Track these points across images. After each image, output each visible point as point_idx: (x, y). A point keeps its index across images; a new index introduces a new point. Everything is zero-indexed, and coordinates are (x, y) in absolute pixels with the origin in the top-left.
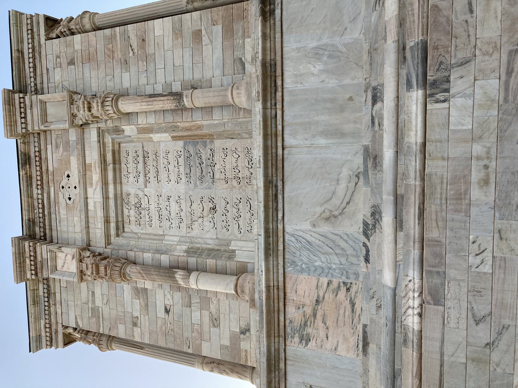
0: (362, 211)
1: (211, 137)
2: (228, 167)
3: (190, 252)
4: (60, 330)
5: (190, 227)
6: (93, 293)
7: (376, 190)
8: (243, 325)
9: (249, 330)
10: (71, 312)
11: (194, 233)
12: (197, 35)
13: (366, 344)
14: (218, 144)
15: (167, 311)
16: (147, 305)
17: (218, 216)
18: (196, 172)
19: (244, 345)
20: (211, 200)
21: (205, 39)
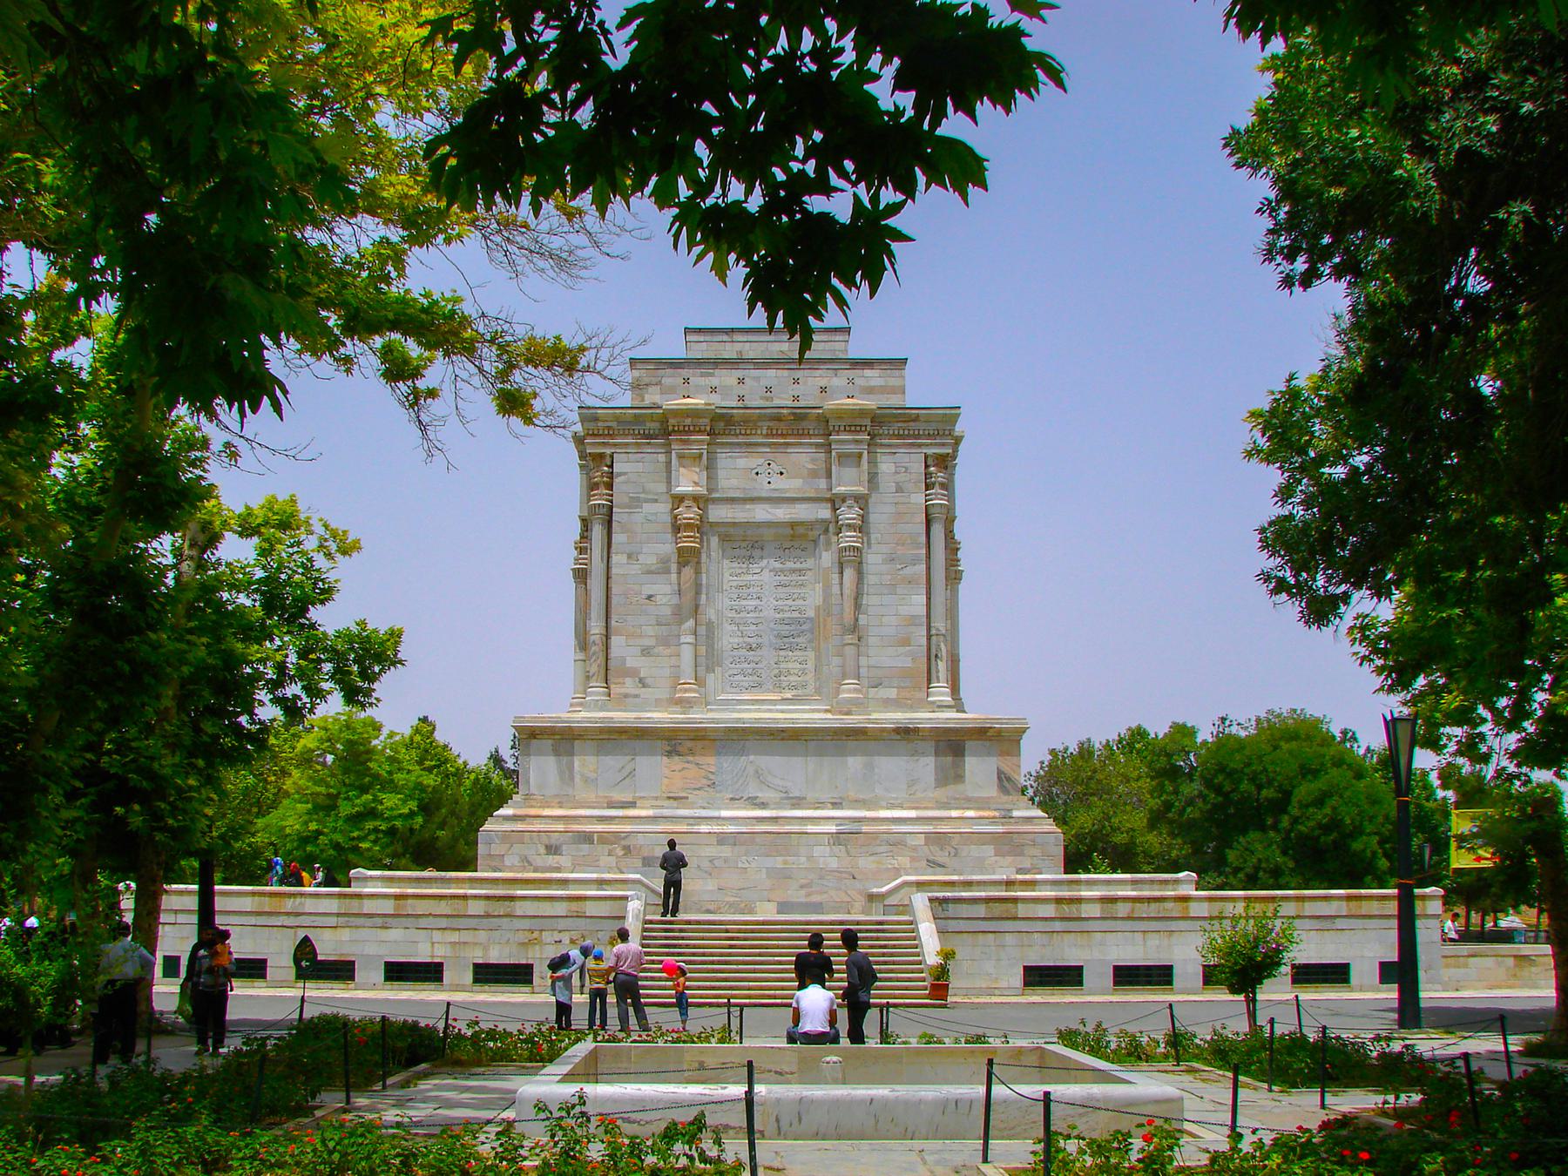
0: (765, 795)
1: (817, 650)
2: (790, 665)
3: (710, 624)
4: (608, 451)
5: (733, 621)
6: (656, 501)
7: (779, 806)
8: (648, 681)
9: (644, 686)
10: (634, 468)
11: (726, 625)
12: (905, 642)
13: (675, 798)
14: (811, 654)
15: (649, 597)
16: (650, 572)
17: (743, 652)
18: (785, 630)
19: (628, 681)
20: (759, 646)
21: (901, 650)
